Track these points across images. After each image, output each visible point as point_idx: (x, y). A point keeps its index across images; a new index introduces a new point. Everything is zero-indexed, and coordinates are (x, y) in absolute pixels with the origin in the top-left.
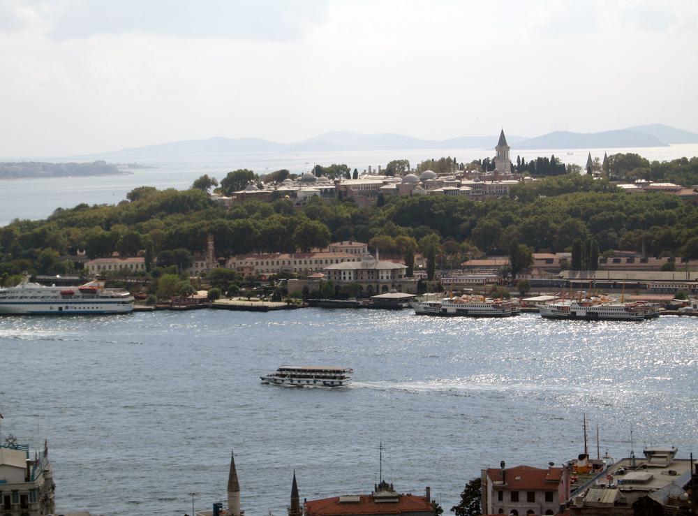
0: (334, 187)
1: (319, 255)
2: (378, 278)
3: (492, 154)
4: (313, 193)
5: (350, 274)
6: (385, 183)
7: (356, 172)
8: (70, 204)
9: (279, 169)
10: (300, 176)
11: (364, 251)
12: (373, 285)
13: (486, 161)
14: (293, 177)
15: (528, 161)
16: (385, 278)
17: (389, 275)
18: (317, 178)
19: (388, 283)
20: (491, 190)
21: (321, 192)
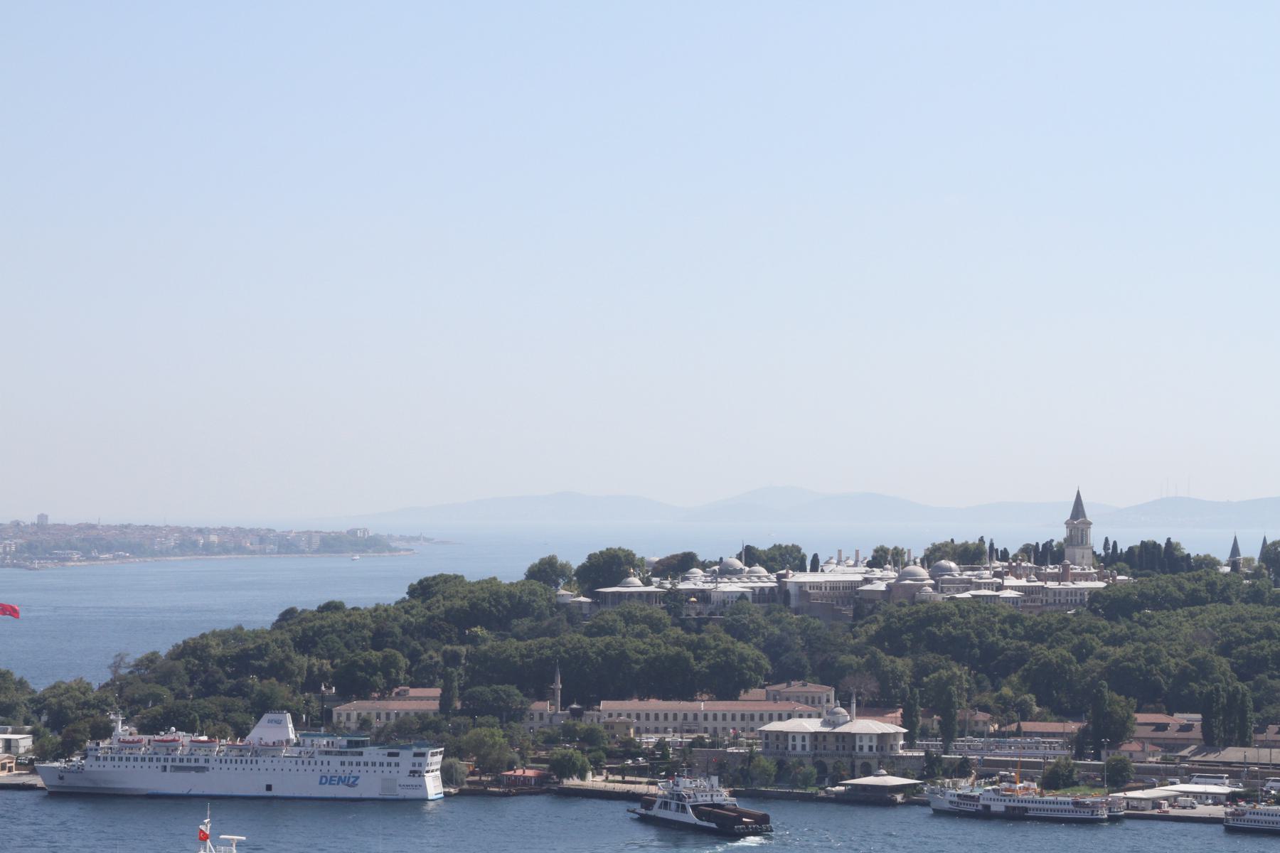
0: (776, 584)
1: (752, 701)
2: (854, 748)
3: (1058, 534)
4: (738, 595)
5: (804, 739)
7: (815, 560)
9: (679, 550)
10: (716, 563)
11: (828, 701)
13: (1048, 546)
14: (704, 566)
15: (1123, 547)
16: (866, 749)
17: (874, 744)
18: (747, 569)
19: (870, 758)
20: (1057, 598)
21: (754, 594)
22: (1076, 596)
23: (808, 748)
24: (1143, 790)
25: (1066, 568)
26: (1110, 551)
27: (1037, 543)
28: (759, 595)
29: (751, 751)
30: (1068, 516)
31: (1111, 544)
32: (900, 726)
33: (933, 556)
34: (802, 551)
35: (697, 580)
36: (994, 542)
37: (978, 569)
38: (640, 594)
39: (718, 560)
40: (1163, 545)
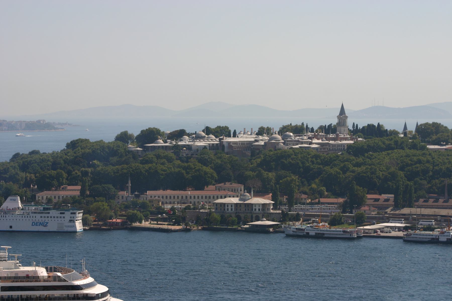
0: (218, 142)
1: (209, 191)
2: (252, 210)
3: (334, 121)
4: (203, 147)
5: (232, 206)
6: (256, 141)
7: (235, 132)
8: (25, 150)
9: (178, 129)
10: (194, 134)
11: (241, 190)
12: (249, 215)
13: (330, 126)
14: (189, 135)
15: (360, 127)
16: (257, 210)
17: (261, 208)
18: (207, 136)
19: (259, 213)
20: (334, 148)
21: (209, 146)
22: (341, 146)
23: (233, 210)
24: (370, 225)
25: (337, 135)
26: (355, 128)
27: (326, 125)
28: (212, 147)
29: (210, 211)
30: (338, 114)
31: (355, 125)
32: (271, 200)
33: (283, 130)
34: (229, 129)
35: (186, 141)
36: (308, 125)
37: (302, 136)
38: (163, 146)
39: (195, 133)
40: (376, 126)
